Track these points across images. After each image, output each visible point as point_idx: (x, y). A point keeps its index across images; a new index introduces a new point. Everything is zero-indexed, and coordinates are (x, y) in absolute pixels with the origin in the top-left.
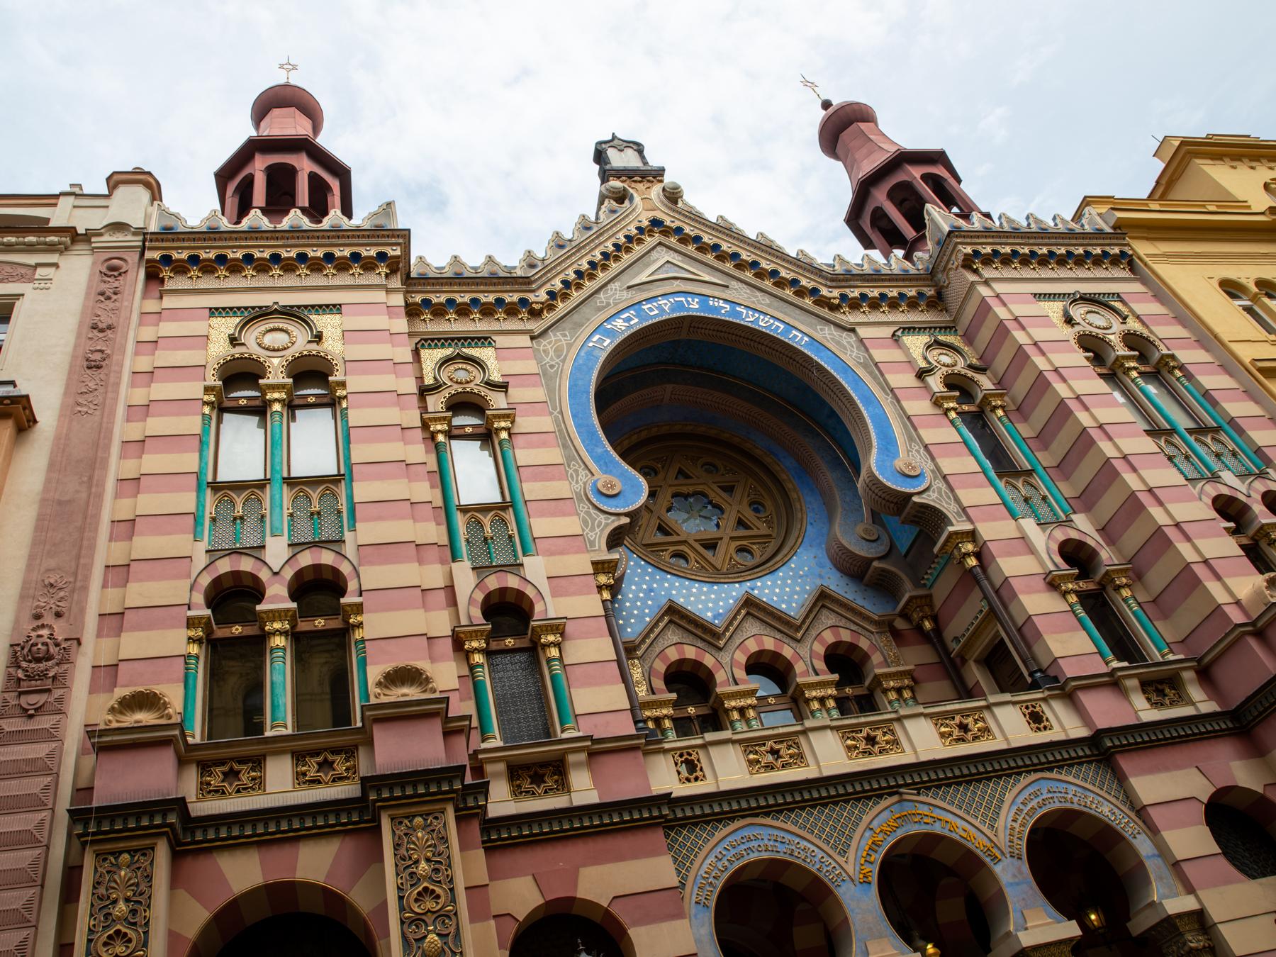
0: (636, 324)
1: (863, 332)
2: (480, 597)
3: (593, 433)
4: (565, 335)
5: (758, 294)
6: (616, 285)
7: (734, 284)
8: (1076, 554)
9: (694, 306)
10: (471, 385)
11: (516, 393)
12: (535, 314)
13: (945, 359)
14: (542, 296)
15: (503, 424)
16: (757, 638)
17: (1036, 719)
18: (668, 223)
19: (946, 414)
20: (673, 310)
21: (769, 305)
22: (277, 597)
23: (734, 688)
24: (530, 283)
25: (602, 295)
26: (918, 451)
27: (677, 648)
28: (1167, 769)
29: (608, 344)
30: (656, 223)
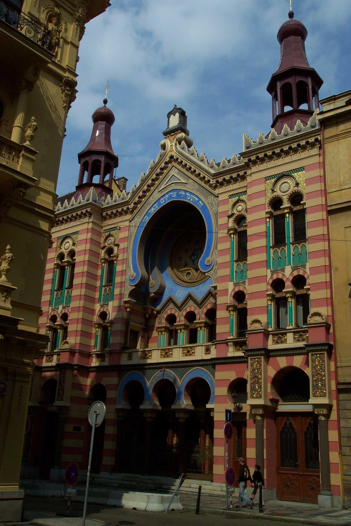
0: (157, 208)
1: (221, 197)
2: (99, 314)
3: (135, 257)
4: (138, 218)
5: (196, 184)
6: (157, 190)
7: (190, 180)
8: (240, 296)
9: (174, 197)
10: (111, 245)
11: (122, 246)
12: (133, 211)
13: (240, 208)
14: (132, 205)
15: (114, 258)
16: (191, 307)
17: (208, 350)
18: (175, 157)
19: (230, 236)
20: (168, 200)
21: (197, 190)
22: (59, 321)
23: (180, 323)
24: (129, 202)
25: (151, 198)
26: (216, 253)
27: (171, 310)
28: (227, 370)
29: (148, 219)
30: (172, 157)
